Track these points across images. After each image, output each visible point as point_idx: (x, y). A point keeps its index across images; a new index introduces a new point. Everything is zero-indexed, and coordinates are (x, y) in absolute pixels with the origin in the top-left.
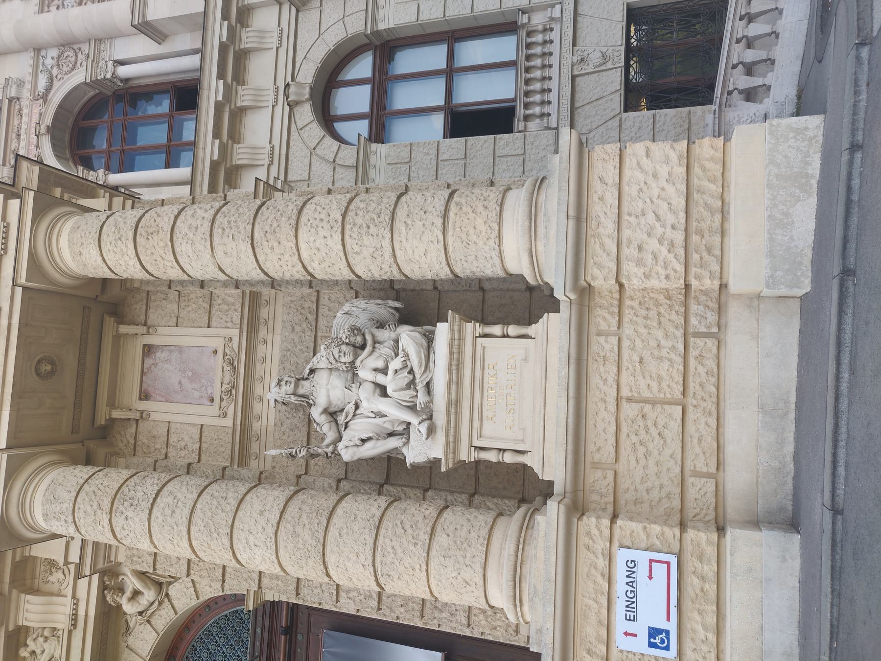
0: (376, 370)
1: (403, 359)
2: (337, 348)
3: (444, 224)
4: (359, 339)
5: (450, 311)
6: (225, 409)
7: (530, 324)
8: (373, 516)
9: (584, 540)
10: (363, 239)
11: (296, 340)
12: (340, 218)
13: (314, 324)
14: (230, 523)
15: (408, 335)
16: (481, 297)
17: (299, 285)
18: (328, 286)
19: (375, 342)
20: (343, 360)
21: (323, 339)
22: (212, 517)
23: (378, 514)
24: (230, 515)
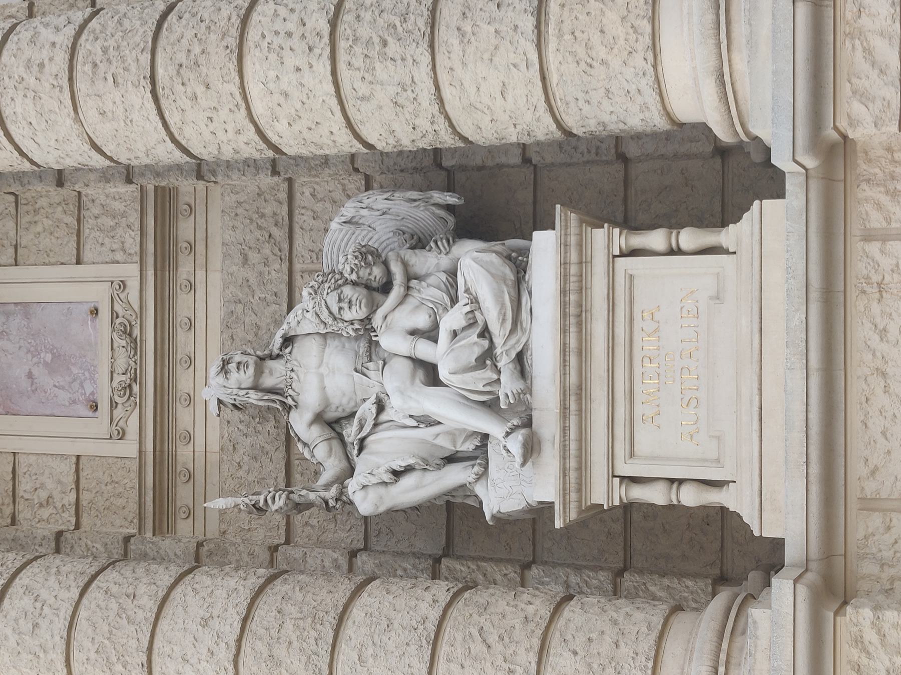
0: (414, 333)
2: (335, 293)
3: (538, 26)
4: (377, 272)
5: (558, 206)
6: (121, 423)
7: (724, 224)
8: (425, 620)
9: (848, 652)
10: (374, 68)
11: (253, 281)
12: (326, 29)
13: (286, 246)
14: (145, 643)
15: (475, 260)
16: (622, 173)
17: (252, 170)
18: (310, 169)
19: (409, 277)
20: (348, 315)
21: (306, 276)
22: (111, 633)
23: (434, 615)
24: (144, 628)
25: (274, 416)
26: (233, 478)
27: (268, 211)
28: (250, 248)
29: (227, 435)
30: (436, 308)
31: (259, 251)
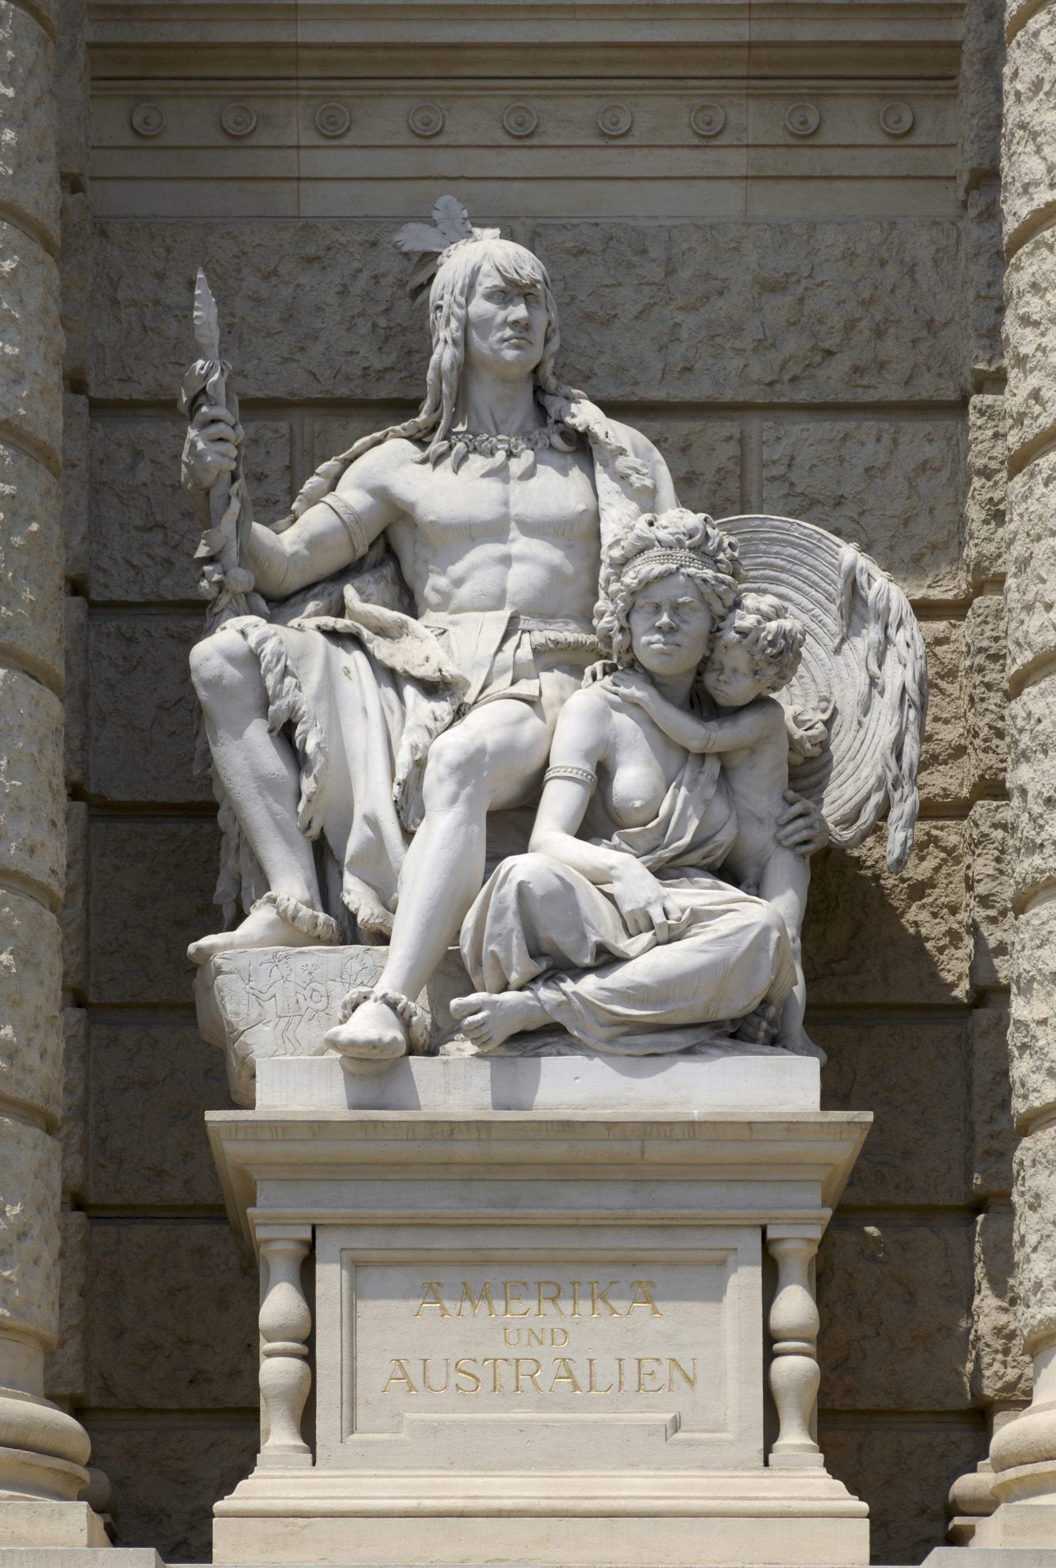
1: (658, 917)
13: (802, 396)
25: (393, 368)
26: (238, 257)
27: (889, 347)
28: (801, 300)
29: (343, 240)
30: (659, 824)
31: (794, 324)
